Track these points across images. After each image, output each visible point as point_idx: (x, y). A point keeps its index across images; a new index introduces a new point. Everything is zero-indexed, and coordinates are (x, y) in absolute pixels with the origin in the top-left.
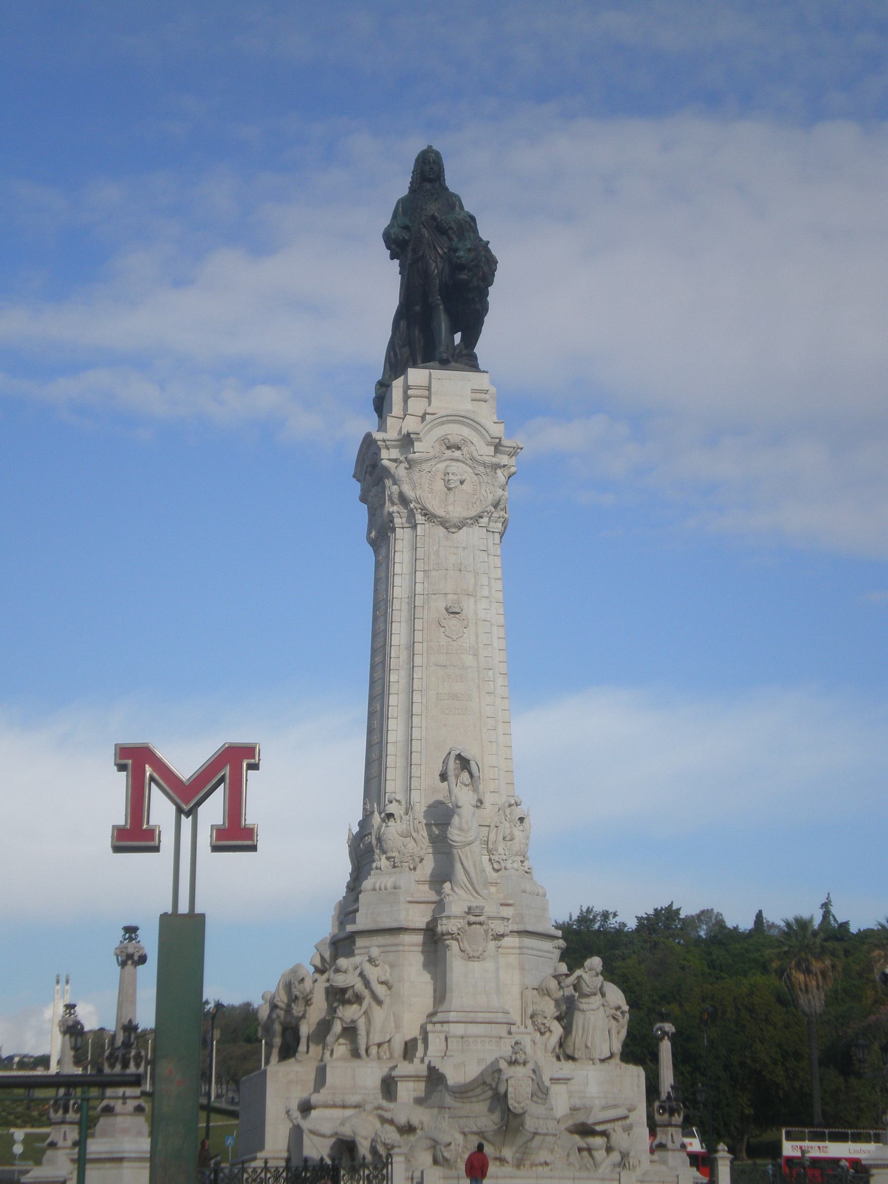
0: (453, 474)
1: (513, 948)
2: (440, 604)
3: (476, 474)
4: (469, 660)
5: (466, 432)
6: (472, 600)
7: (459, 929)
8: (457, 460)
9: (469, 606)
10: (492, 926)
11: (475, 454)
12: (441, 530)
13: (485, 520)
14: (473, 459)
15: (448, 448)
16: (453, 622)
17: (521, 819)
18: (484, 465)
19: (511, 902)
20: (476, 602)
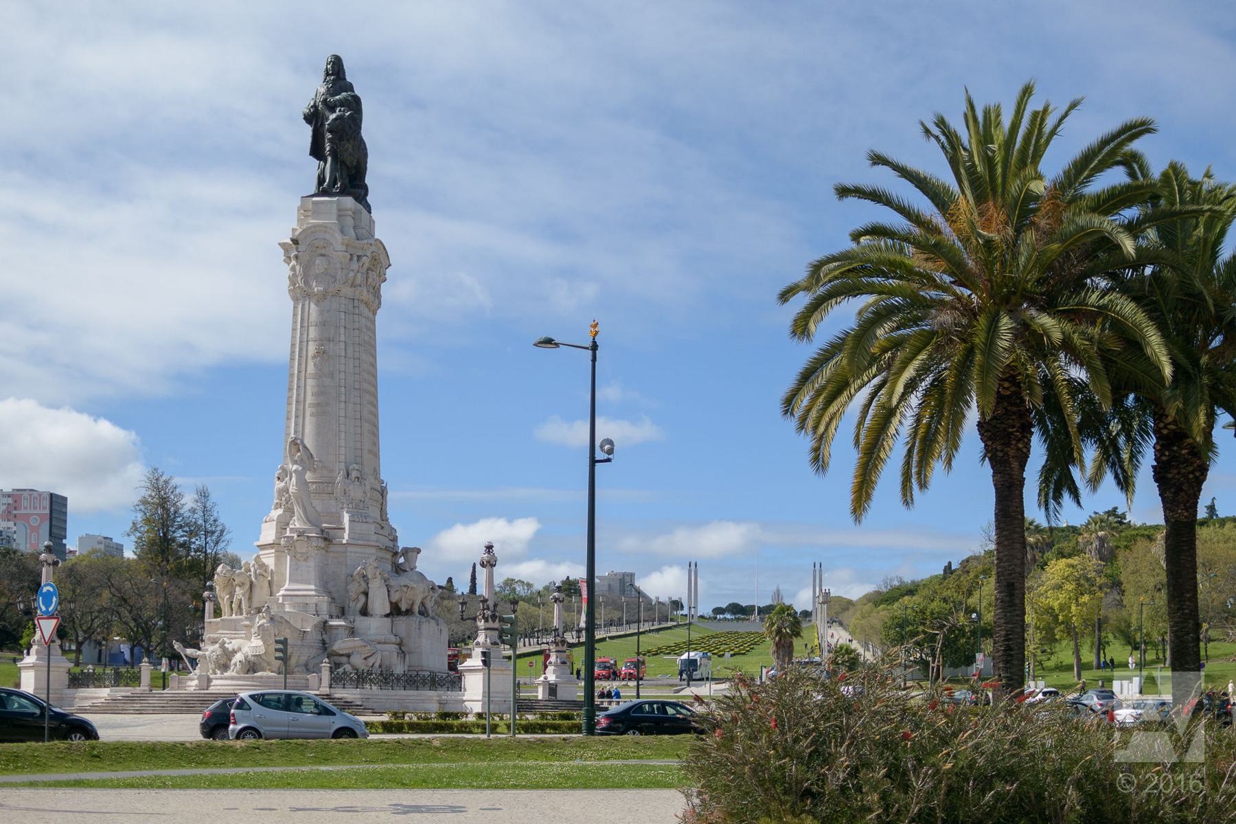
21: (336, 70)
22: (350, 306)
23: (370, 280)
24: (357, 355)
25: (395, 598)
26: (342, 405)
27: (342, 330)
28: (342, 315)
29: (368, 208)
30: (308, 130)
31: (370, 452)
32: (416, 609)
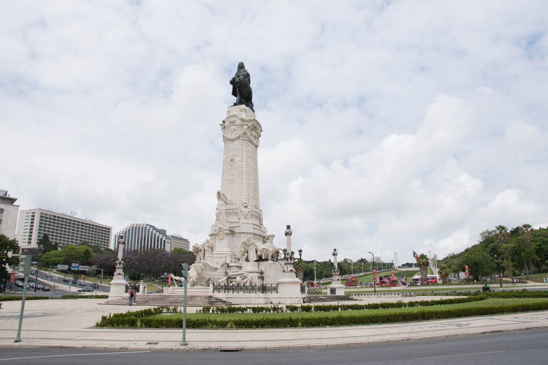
2: (229, 159)
4: (235, 171)
5: (235, 118)
9: (236, 159)
13: (241, 138)
16: (232, 163)
17: (246, 207)
21: (241, 66)
25: (259, 253)
26: (240, 179)
29: (254, 111)
30: (231, 86)
31: (253, 197)
32: (269, 258)
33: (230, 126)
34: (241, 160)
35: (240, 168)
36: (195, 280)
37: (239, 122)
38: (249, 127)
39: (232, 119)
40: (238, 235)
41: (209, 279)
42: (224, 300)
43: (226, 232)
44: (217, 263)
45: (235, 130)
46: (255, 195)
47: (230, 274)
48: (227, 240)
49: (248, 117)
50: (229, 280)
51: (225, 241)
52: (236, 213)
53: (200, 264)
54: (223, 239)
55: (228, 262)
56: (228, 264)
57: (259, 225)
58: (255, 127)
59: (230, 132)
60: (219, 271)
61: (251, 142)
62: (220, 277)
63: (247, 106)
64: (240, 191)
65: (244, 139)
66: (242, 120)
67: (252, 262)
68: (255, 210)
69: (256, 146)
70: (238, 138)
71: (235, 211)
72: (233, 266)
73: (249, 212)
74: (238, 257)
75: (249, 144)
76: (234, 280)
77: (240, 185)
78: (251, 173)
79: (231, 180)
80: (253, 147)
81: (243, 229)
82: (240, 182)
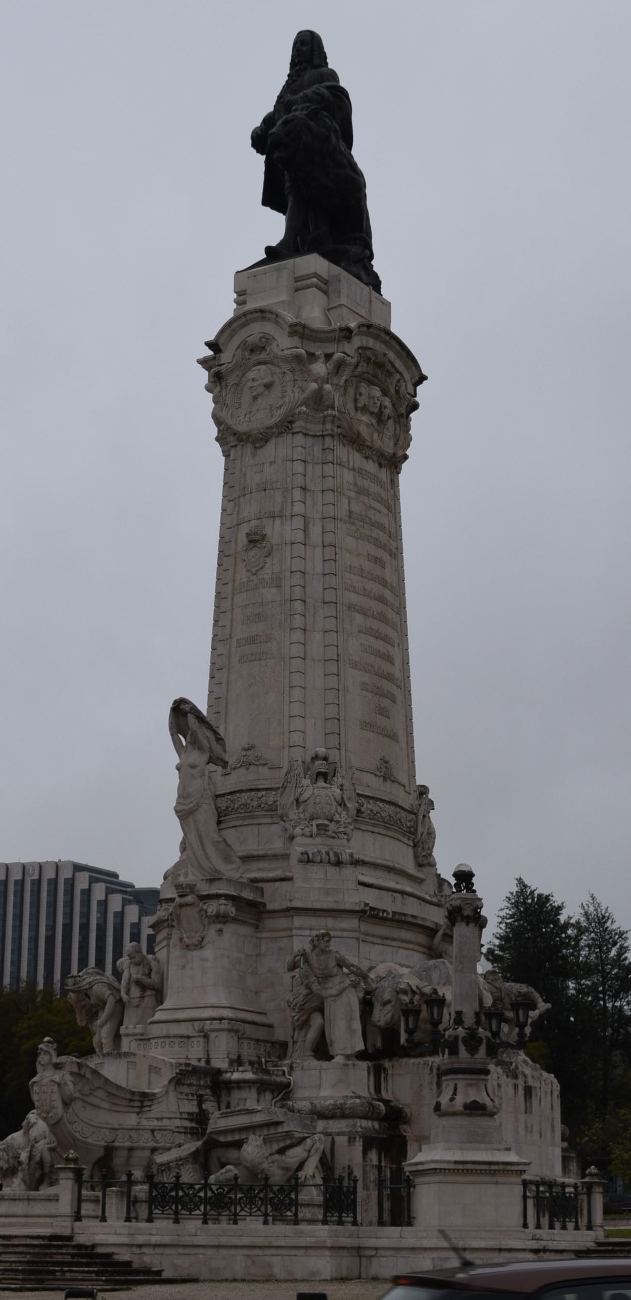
0: (253, 380)
1: (285, 930)
3: (284, 373)
4: (269, 594)
5: (268, 328)
6: (278, 521)
7: (171, 914)
8: (264, 363)
9: (274, 531)
10: (205, 907)
11: (275, 350)
12: (249, 448)
13: (297, 424)
14: (276, 357)
15: (252, 351)
18: (285, 359)
19: (289, 874)
20: (282, 523)
21: (308, 51)
22: (317, 451)
23: (363, 401)
24: (329, 538)
25: (381, 1016)
26: (298, 636)
27: (297, 494)
28: (299, 467)
29: (375, 283)
31: (366, 725)
33: (242, 367)
34: (300, 536)
35: (297, 579)
36: (47, 1157)
37: (284, 344)
38: (339, 366)
39: (256, 330)
40: (282, 922)
41: (110, 1150)
42: (124, 1256)
43: (212, 908)
44: (154, 1069)
45: (268, 386)
46: (384, 712)
47: (218, 1122)
48: (223, 948)
49: (333, 315)
50: (215, 1154)
51: (208, 952)
52: (272, 808)
53: (57, 1077)
54: (200, 945)
55: (220, 1062)
56: (219, 1072)
57: (411, 868)
58: (380, 365)
59: (246, 398)
60: (158, 1109)
61: (355, 441)
62: (162, 1140)
63: (333, 257)
64: (297, 694)
65: (317, 429)
66: (300, 331)
67: (339, 1059)
68: (373, 785)
69: (394, 462)
70: (286, 426)
71: (271, 798)
72: (240, 1084)
73: (342, 803)
74: (280, 1034)
75: (344, 452)
76: (233, 1154)
77: (297, 664)
78: (354, 598)
79: (252, 640)
80: (371, 467)
81: (310, 887)
82: (297, 650)
